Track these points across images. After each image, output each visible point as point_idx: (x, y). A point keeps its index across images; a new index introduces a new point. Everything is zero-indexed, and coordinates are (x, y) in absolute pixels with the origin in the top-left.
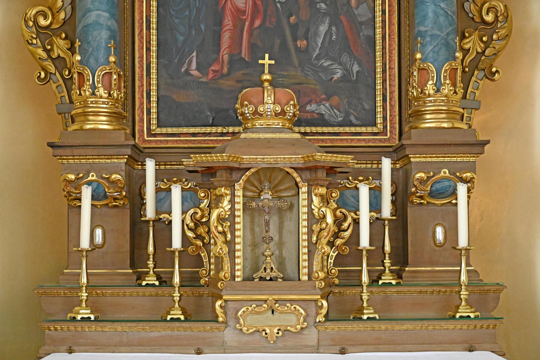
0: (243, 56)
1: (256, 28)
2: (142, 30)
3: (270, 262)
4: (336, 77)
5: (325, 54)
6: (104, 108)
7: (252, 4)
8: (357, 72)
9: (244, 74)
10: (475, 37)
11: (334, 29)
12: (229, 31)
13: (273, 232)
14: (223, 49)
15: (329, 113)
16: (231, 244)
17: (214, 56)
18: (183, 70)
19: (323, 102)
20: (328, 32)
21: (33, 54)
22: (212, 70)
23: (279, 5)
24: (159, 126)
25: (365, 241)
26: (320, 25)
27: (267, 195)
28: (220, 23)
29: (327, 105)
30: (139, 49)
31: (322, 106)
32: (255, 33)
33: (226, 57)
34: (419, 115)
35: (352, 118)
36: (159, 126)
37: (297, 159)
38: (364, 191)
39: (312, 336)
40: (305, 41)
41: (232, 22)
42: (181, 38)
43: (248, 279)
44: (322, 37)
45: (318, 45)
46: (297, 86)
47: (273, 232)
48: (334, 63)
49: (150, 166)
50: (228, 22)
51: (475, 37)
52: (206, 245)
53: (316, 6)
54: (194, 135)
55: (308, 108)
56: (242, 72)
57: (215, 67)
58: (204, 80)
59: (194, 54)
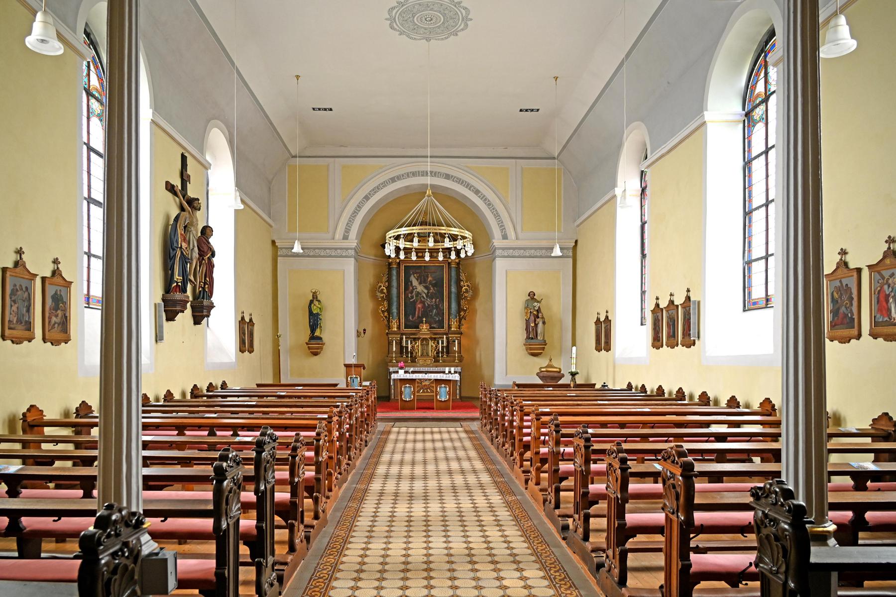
3: (425, 353)
5: (435, 315)
6: (396, 326)
13: (426, 348)
16: (418, 350)
20: (436, 312)
25: (440, 350)
27: (424, 342)
28: (415, 310)
34: (451, 328)
37: (429, 336)
38: (440, 342)
39: (431, 365)
43: (421, 356)
47: (426, 348)
49: (404, 337)
50: (417, 310)
52: (414, 351)
57: (415, 318)
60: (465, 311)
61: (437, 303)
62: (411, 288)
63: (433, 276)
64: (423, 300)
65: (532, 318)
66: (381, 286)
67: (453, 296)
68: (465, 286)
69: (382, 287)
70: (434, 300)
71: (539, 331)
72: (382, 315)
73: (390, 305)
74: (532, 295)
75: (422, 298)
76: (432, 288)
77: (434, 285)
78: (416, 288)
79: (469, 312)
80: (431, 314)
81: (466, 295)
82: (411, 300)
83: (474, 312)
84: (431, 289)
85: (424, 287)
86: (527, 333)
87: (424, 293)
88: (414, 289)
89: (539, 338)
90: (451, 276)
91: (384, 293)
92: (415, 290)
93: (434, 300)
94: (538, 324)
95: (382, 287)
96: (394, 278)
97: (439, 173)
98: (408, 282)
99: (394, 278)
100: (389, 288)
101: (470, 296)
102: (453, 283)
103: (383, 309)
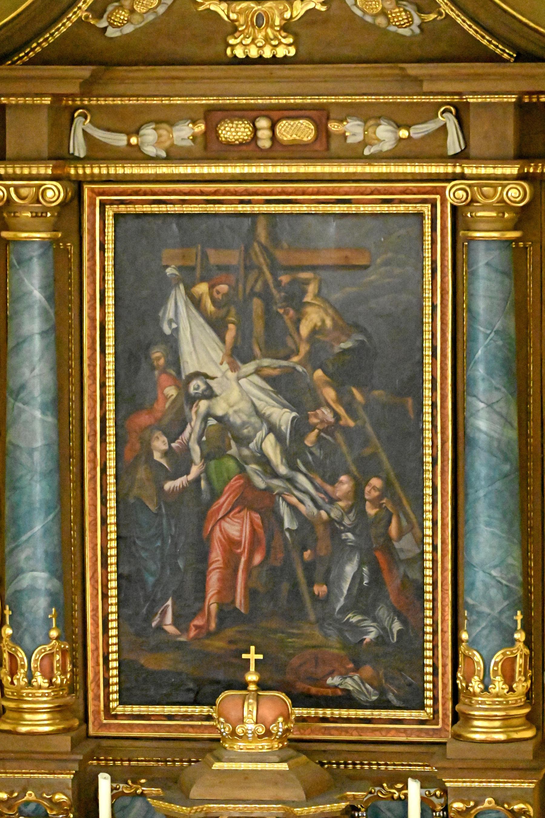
0: (238, 605)
1: (256, 567)
2: (96, 571)
4: (369, 638)
7: (250, 532)
8: (399, 632)
9: (240, 632)
11: (365, 569)
12: (218, 570)
14: (209, 596)
15: (357, 688)
17: (198, 605)
18: (154, 624)
19: (351, 674)
20: (358, 575)
22: (195, 626)
23: (288, 535)
24: (122, 702)
26: (346, 563)
29: (356, 678)
30: (92, 598)
31: (348, 680)
32: (255, 573)
33: (214, 608)
35: (391, 697)
36: (122, 702)
40: (325, 587)
41: (223, 558)
42: (151, 580)
44: (349, 580)
45: (342, 593)
46: (313, 651)
48: (366, 618)
53: (341, 536)
54: (170, 717)
55: (329, 681)
56: (236, 628)
57: (198, 622)
58: (182, 639)
59: (169, 602)
61: (371, 511)
62: (171, 391)
63: (336, 296)
64: (260, 482)
75: (252, 468)
76: (330, 394)
80: (320, 589)
82: (169, 485)
84: (319, 402)
85: (267, 379)
87: (272, 429)
88: (192, 400)
92: (203, 405)
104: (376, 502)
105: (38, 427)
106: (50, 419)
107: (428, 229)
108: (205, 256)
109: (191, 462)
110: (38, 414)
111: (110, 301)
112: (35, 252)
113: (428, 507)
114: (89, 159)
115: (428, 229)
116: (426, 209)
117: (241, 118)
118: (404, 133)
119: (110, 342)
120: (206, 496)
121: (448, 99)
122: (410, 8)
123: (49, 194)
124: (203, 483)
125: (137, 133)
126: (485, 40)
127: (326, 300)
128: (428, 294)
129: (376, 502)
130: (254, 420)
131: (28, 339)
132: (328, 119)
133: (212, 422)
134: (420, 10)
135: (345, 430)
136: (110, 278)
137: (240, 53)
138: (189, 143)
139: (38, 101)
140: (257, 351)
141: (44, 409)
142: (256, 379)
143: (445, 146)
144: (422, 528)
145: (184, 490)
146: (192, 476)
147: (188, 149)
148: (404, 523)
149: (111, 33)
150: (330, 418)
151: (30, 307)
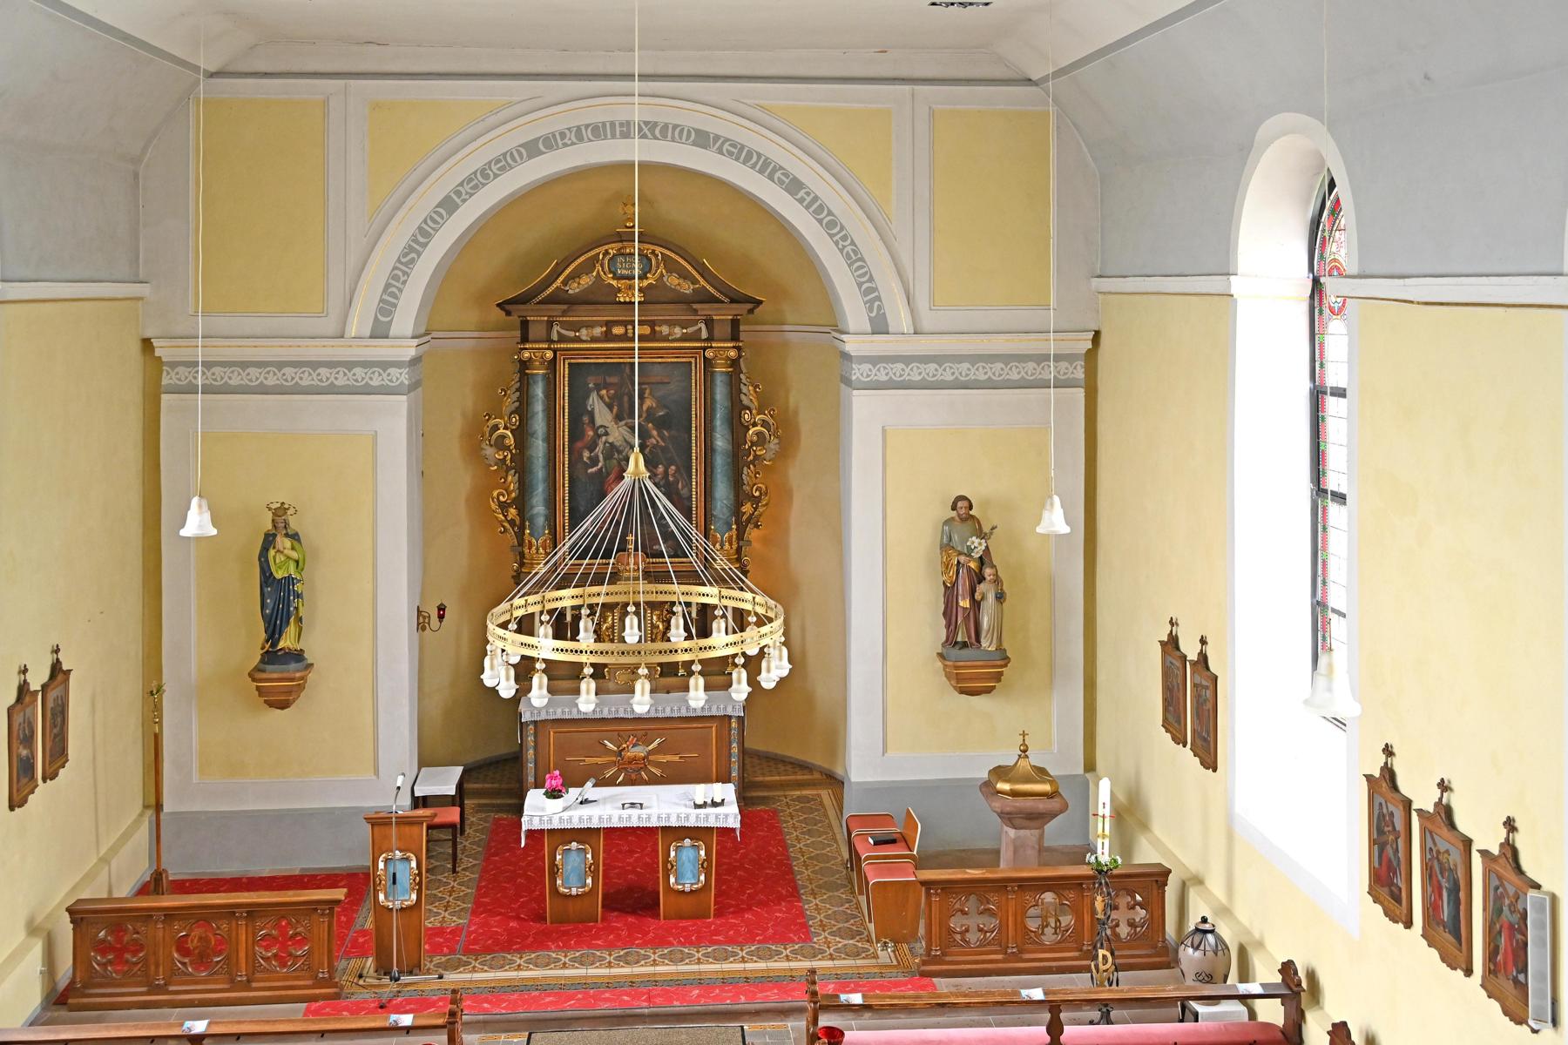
10: (749, 505)
21: (497, 518)
51: (749, 505)
60: (757, 500)
61: (671, 479)
62: (591, 433)
63: (658, 394)
65: (963, 585)
66: (496, 428)
67: (720, 461)
68: (755, 425)
69: (501, 431)
70: (661, 469)
71: (985, 622)
72: (501, 516)
73: (524, 488)
74: (961, 504)
76: (655, 433)
77: (661, 424)
78: (607, 434)
79: (766, 504)
81: (758, 453)
82: (590, 471)
83: (786, 494)
84: (651, 436)
86: (948, 626)
88: (599, 436)
89: (985, 643)
90: (713, 400)
91: (508, 448)
92: (604, 438)
93: (661, 469)
94: (982, 599)
95: (501, 431)
96: (539, 407)
97: (675, 127)
98: (579, 413)
99: (539, 407)
100: (522, 433)
101: (770, 455)
102: (718, 423)
103: (501, 498)
104: (673, 475)
105: (541, 448)
106: (545, 445)
107: (693, 368)
108: (605, 378)
109: (599, 461)
110: (541, 442)
111: (566, 398)
112: (540, 378)
113: (694, 477)
114: (559, 341)
115: (693, 368)
116: (693, 360)
117: (621, 325)
118: (685, 331)
119: (566, 414)
120: (605, 474)
121: (702, 318)
122: (689, 283)
123: (548, 355)
124: (604, 470)
125: (578, 331)
126: (718, 295)
127: (653, 396)
128: (693, 393)
129: (673, 475)
130: (624, 444)
131: (537, 413)
132: (655, 325)
133: (607, 445)
134: (693, 283)
135: (661, 447)
136: (567, 388)
137: (622, 300)
138: (599, 335)
139: (542, 318)
140: (625, 416)
141: (543, 441)
142: (625, 427)
143: (701, 335)
144: (691, 485)
145: (596, 473)
146: (599, 467)
147: (599, 338)
148: (684, 483)
149: (570, 292)
150: (655, 442)
151: (538, 400)
